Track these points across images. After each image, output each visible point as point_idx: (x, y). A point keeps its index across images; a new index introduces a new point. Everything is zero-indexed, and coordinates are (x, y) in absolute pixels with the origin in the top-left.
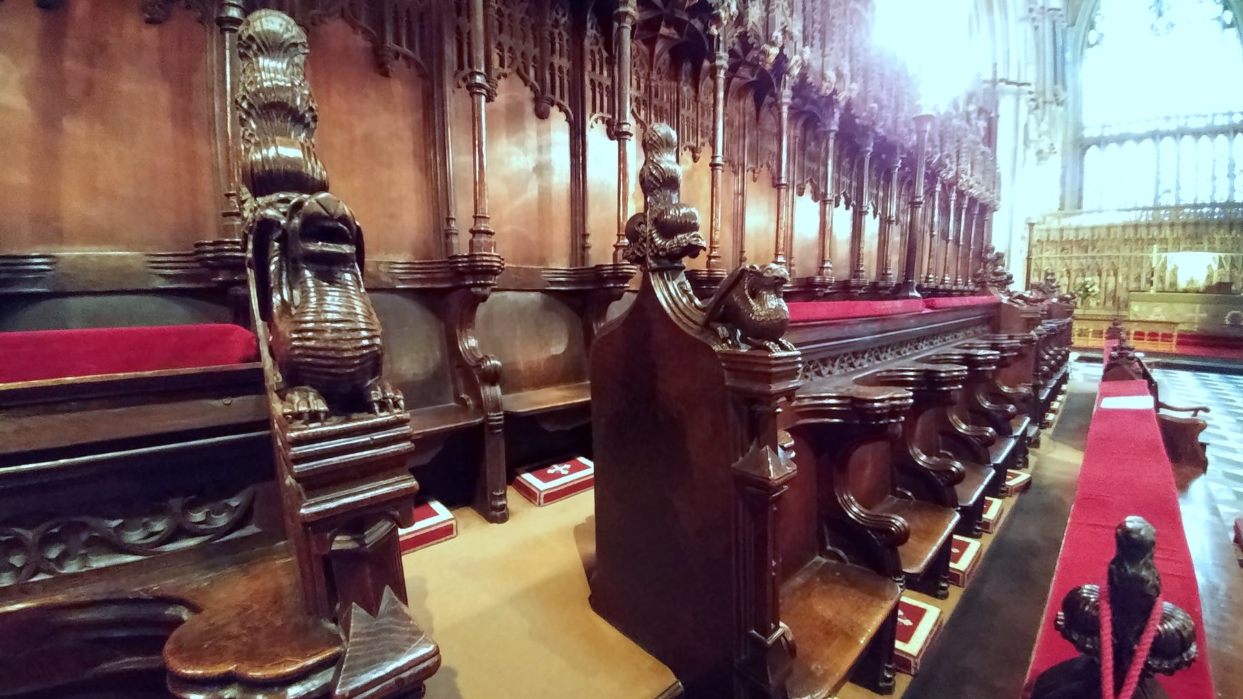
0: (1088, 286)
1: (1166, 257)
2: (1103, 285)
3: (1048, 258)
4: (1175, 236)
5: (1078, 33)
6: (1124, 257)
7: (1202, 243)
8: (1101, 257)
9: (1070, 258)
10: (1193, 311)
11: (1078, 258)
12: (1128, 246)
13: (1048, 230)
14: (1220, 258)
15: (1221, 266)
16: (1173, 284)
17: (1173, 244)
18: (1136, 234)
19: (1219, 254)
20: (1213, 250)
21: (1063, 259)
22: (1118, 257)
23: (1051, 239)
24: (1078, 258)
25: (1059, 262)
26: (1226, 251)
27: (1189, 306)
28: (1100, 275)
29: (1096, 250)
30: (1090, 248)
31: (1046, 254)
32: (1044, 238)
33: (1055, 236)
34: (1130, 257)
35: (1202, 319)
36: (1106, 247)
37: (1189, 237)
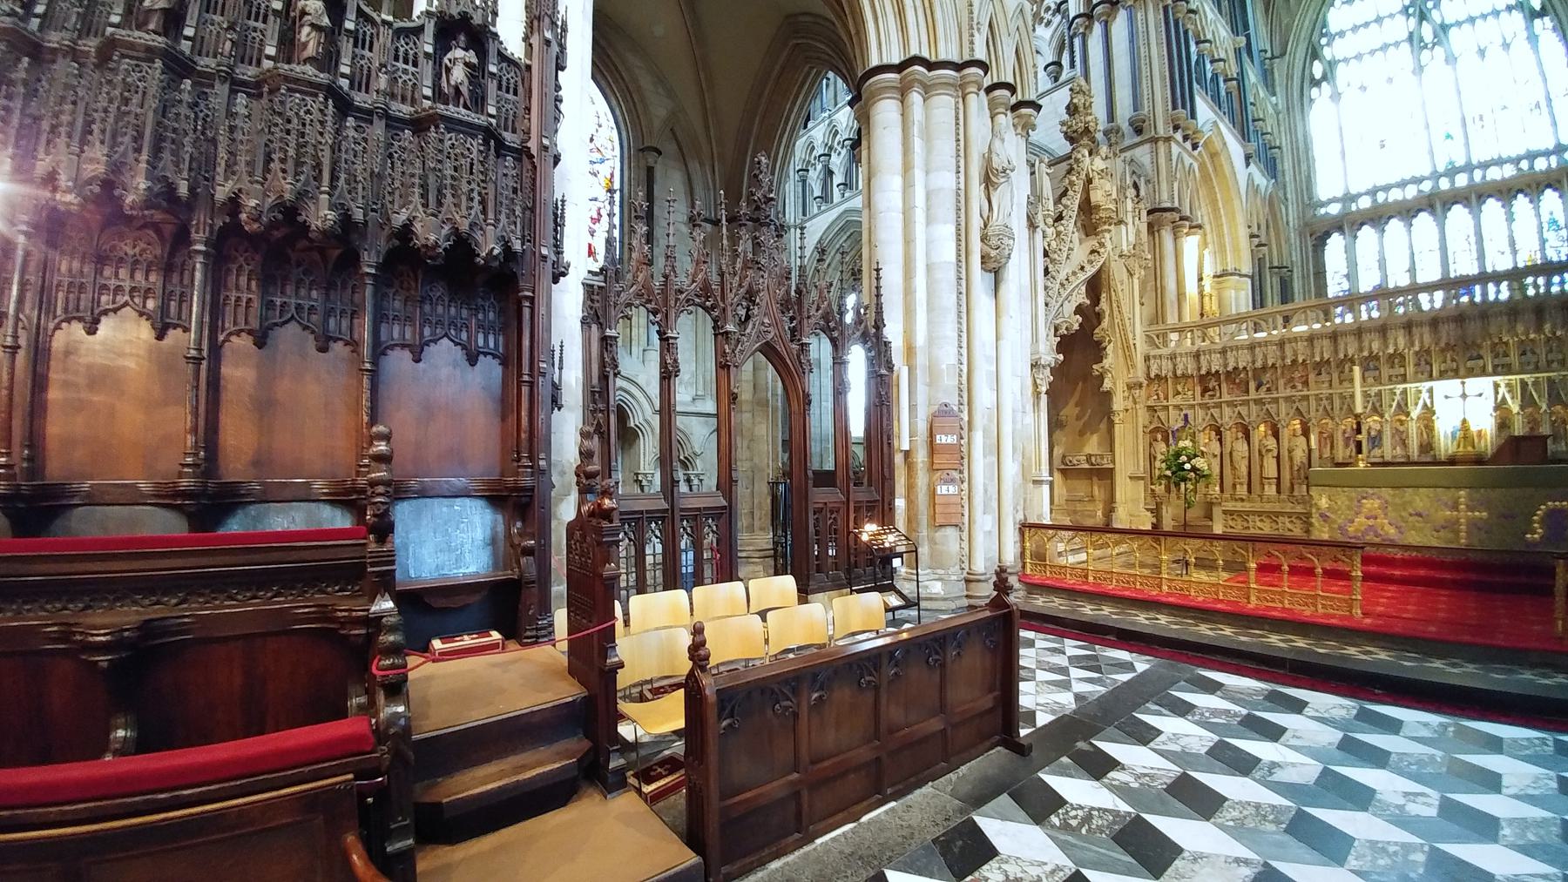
0: (1183, 458)
1: (1405, 392)
2: (1285, 453)
3: (1178, 407)
4: (1417, 348)
5: (1290, 67)
6: (1318, 399)
7: (1480, 357)
8: (1276, 400)
9: (1219, 406)
10: (1455, 507)
11: (1231, 404)
12: (1324, 377)
13: (1173, 357)
14: (1524, 384)
15: (1527, 401)
16: (1427, 446)
17: (1417, 365)
18: (1336, 352)
19: (1518, 377)
20: (1507, 369)
22: (1306, 398)
23: (1179, 372)
24: (1231, 404)
25: (1200, 413)
26: (1537, 369)
27: (1446, 495)
30: (1252, 385)
31: (1178, 400)
34: (1330, 398)
35: (1473, 525)
36: (1281, 382)
37: (1449, 347)
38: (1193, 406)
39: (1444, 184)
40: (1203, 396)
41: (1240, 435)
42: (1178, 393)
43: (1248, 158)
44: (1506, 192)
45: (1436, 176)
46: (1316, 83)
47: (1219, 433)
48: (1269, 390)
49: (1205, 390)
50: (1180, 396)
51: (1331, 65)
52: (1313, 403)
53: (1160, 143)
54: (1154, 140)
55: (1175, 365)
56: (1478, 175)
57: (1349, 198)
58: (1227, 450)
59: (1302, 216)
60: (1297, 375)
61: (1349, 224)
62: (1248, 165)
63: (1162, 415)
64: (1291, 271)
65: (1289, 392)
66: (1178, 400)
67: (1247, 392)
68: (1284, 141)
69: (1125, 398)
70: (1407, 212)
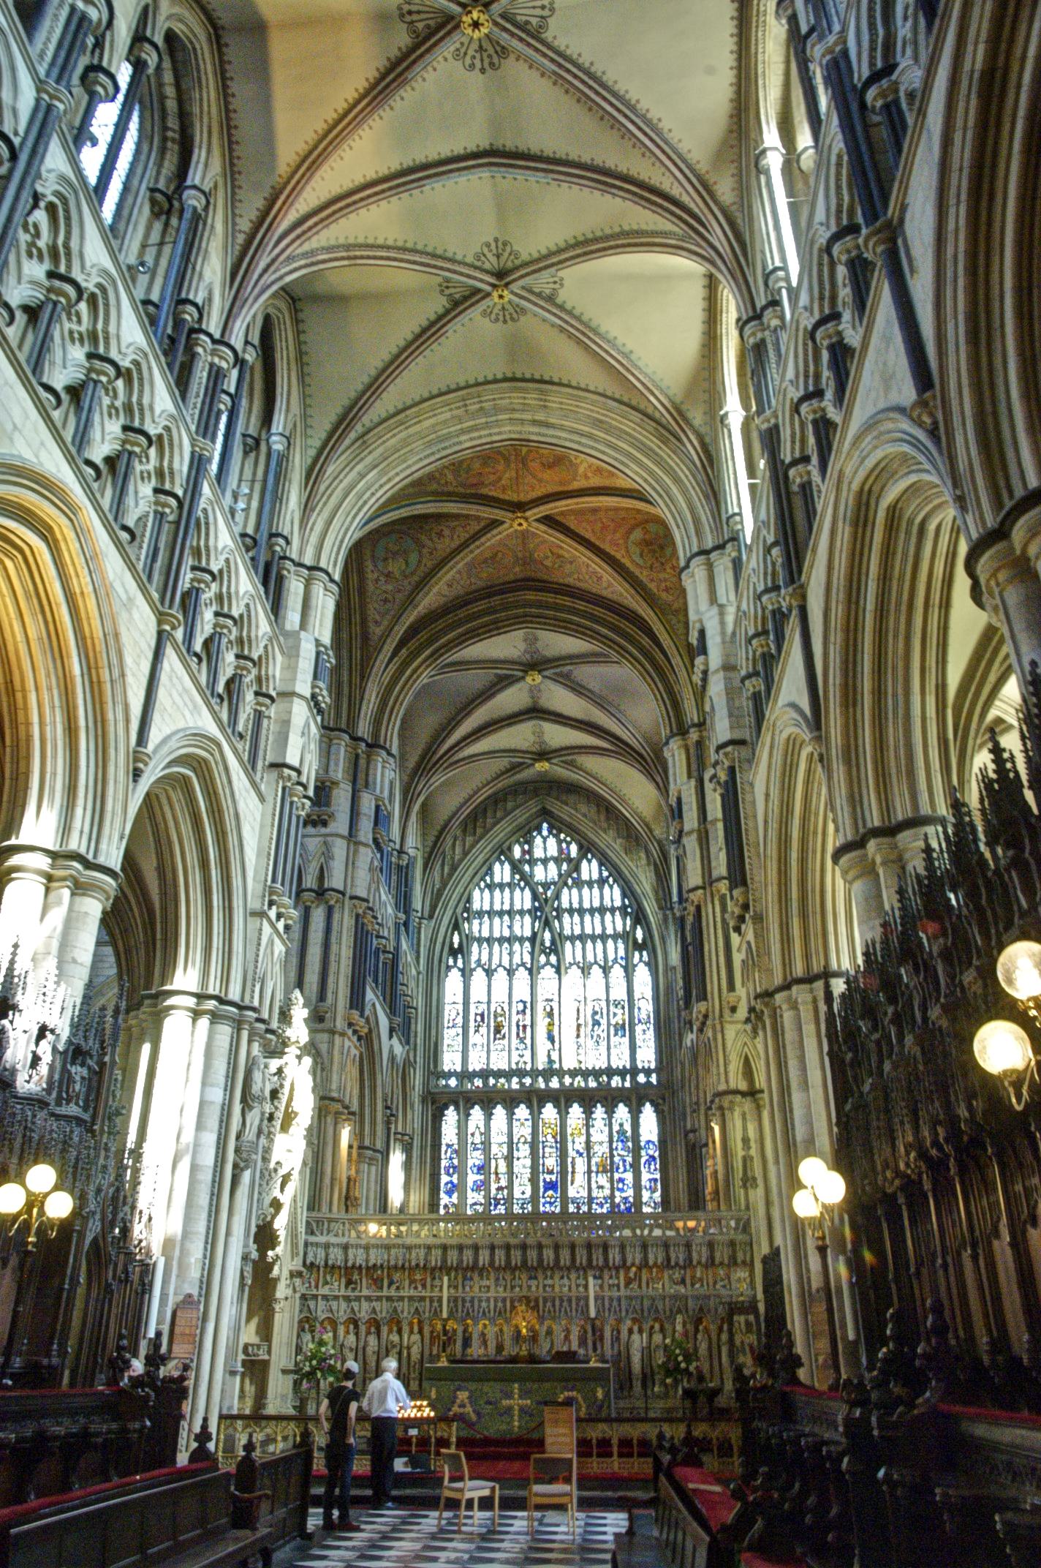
3: (325, 1297)
8: (401, 1299)
11: (368, 1299)
21: (347, 1299)
22: (422, 1299)
23: (330, 1262)
24: (368, 1299)
25: (343, 1305)
28: (400, 1332)
29: (394, 1287)
32: (320, 1261)
33: (336, 1256)
38: (336, 1298)
39: (541, 1084)
40: (346, 1287)
41: (373, 1330)
42: (326, 1283)
43: (392, 1030)
44: (588, 1100)
45: (534, 1073)
46: (454, 953)
47: (356, 1327)
48: (398, 1288)
49: (349, 1282)
50: (327, 1287)
51: (468, 939)
52: (428, 1303)
53: (337, 1037)
54: (332, 1032)
55: (327, 1255)
56: (567, 1080)
57: (465, 1075)
58: (361, 1344)
59: (426, 1084)
60: (418, 1277)
61: (464, 1101)
62: (391, 1037)
63: (312, 1304)
64: (412, 1139)
65: (412, 1292)
66: (324, 1291)
67: (381, 1288)
68: (419, 1002)
69: (288, 1286)
70: (510, 1101)
